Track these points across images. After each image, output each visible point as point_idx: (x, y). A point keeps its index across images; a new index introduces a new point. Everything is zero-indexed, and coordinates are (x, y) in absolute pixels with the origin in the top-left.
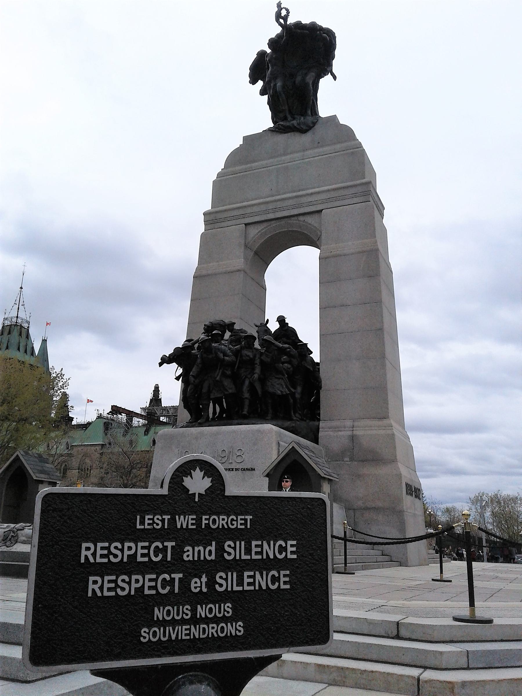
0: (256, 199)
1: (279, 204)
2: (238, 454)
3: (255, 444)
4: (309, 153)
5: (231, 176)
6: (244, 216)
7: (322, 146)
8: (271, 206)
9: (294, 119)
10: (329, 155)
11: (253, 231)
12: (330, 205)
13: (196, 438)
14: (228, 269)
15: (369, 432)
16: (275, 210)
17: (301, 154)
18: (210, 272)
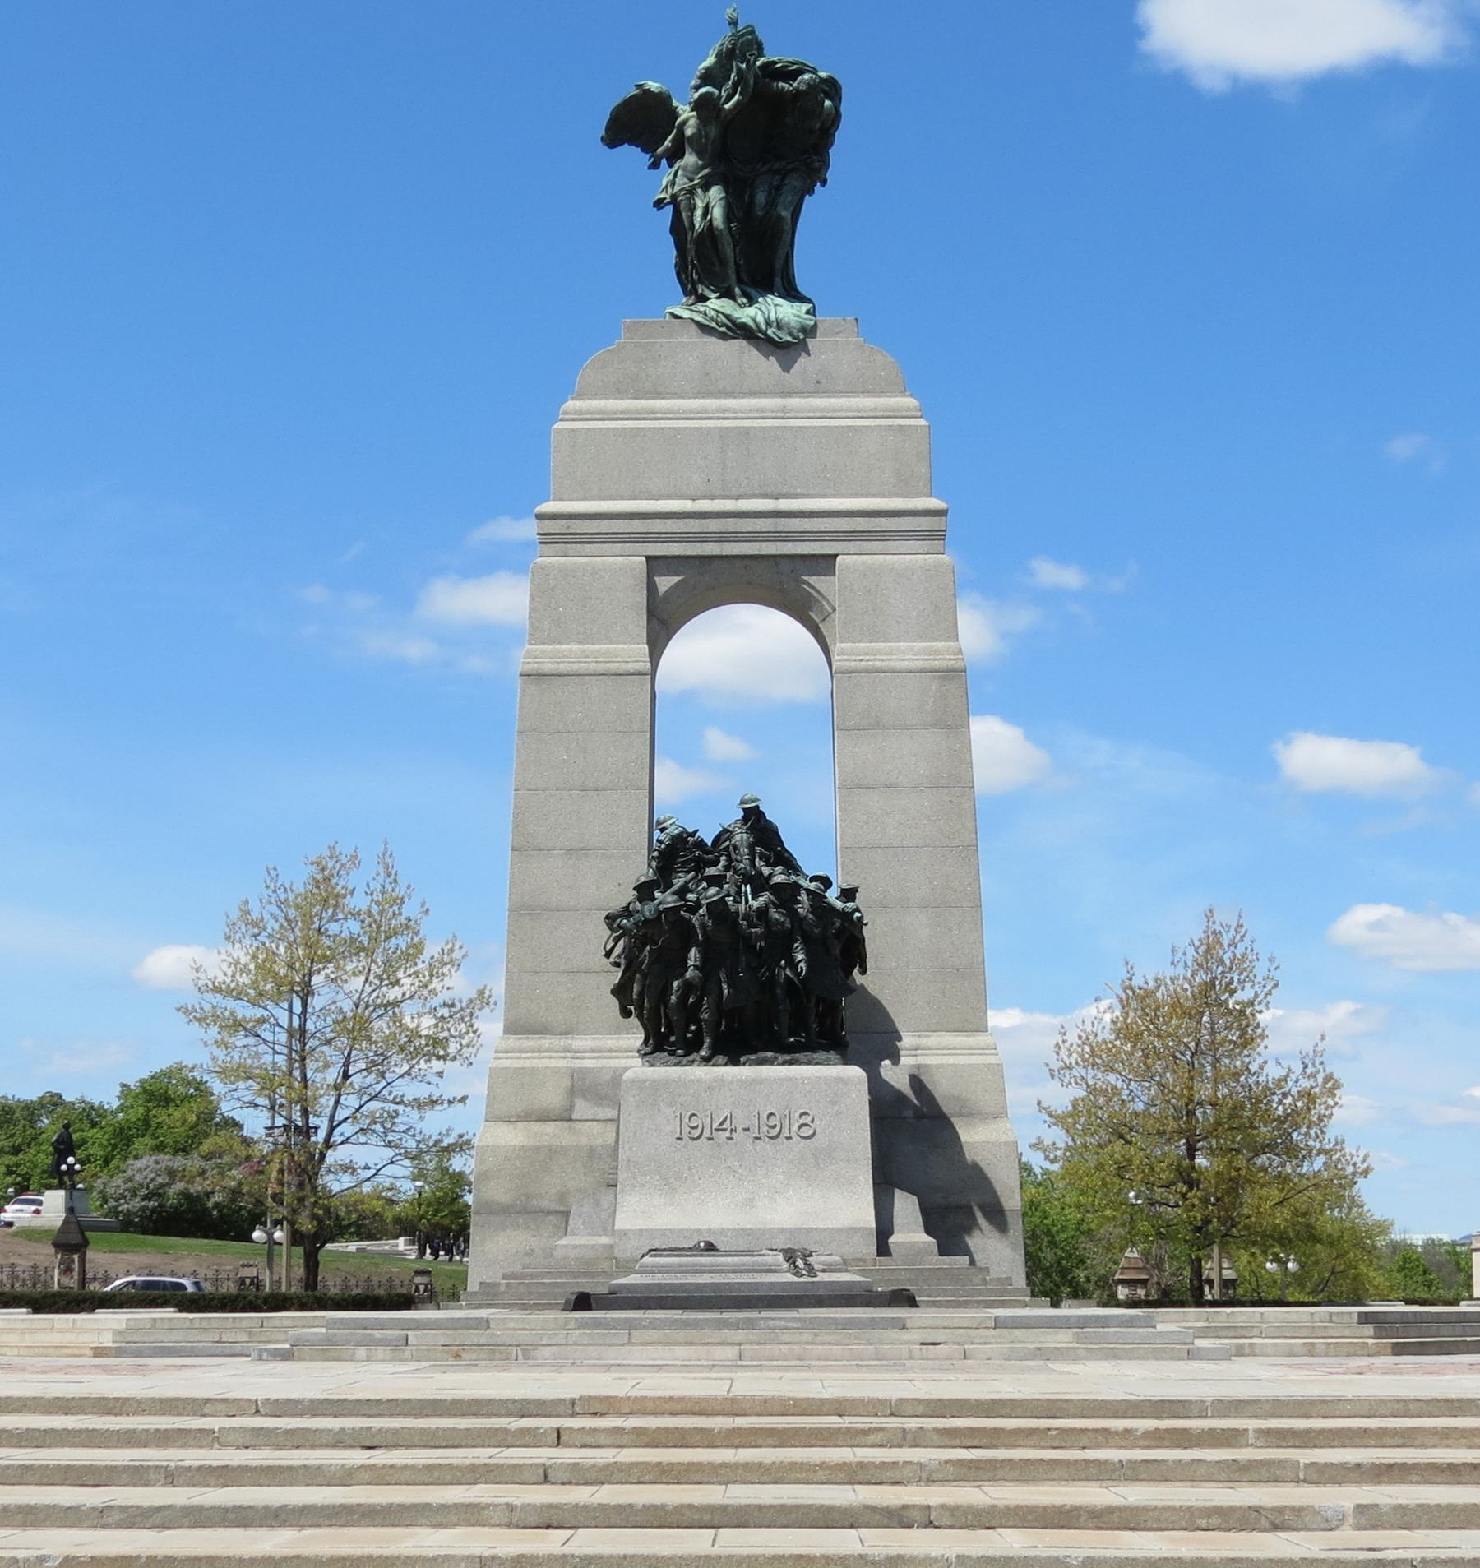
0: (669, 497)
1: (731, 525)
2: (802, 1121)
3: (833, 1103)
4: (794, 402)
5: (600, 424)
6: (644, 538)
8: (713, 525)
9: (752, 301)
10: (849, 422)
12: (852, 546)
13: (710, 1088)
14: (614, 667)
15: (951, 1060)
16: (722, 537)
17: (777, 402)
18: (563, 668)
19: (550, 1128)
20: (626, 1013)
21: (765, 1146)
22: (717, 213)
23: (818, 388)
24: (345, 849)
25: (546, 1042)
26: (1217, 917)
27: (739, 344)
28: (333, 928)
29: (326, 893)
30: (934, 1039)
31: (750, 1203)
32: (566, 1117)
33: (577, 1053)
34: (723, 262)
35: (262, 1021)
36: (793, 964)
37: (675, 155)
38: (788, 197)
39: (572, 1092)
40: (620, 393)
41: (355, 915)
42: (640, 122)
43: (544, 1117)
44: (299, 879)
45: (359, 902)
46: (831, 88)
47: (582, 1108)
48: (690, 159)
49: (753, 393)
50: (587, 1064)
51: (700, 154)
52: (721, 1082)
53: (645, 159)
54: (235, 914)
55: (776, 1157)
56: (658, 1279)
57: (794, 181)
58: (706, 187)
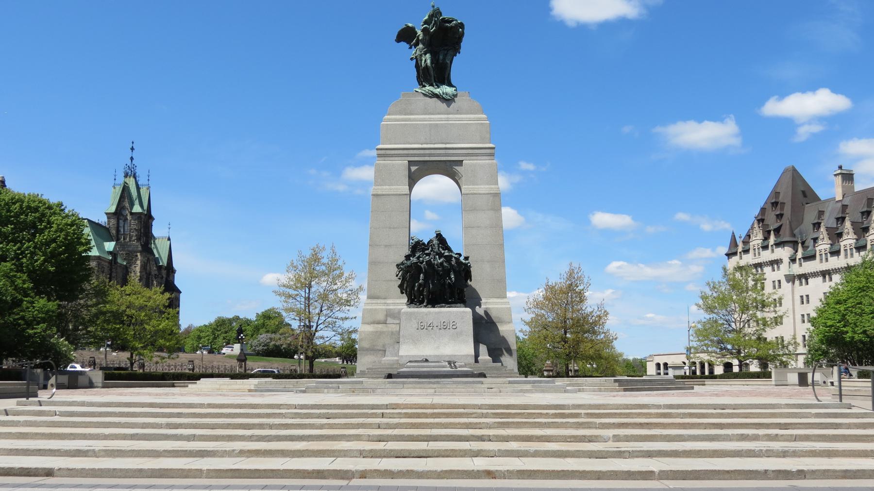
1: (433, 152)
4: (451, 116)
6: (407, 155)
7: (461, 114)
8: (427, 152)
11: (413, 168)
16: (430, 155)
19: (380, 326)
20: (402, 293)
21: (443, 331)
22: (429, 62)
23: (458, 112)
24: (321, 245)
25: (379, 301)
26: (573, 265)
27: (435, 99)
28: (318, 268)
29: (316, 258)
30: (491, 300)
31: (438, 347)
32: (385, 323)
33: (388, 304)
34: (430, 76)
35: (297, 295)
36: (450, 279)
37: (416, 45)
38: (449, 57)
39: (387, 316)
40: (401, 114)
41: (324, 264)
42: (406, 35)
43: (379, 323)
44: (308, 254)
45: (325, 261)
46: (461, 25)
47: (389, 320)
48: (421, 46)
49: (439, 114)
50: (391, 307)
51: (424, 44)
52: (430, 313)
53: (408, 46)
54: (289, 264)
55: (446, 335)
56: (412, 369)
57: (451, 52)
58: (425, 54)
